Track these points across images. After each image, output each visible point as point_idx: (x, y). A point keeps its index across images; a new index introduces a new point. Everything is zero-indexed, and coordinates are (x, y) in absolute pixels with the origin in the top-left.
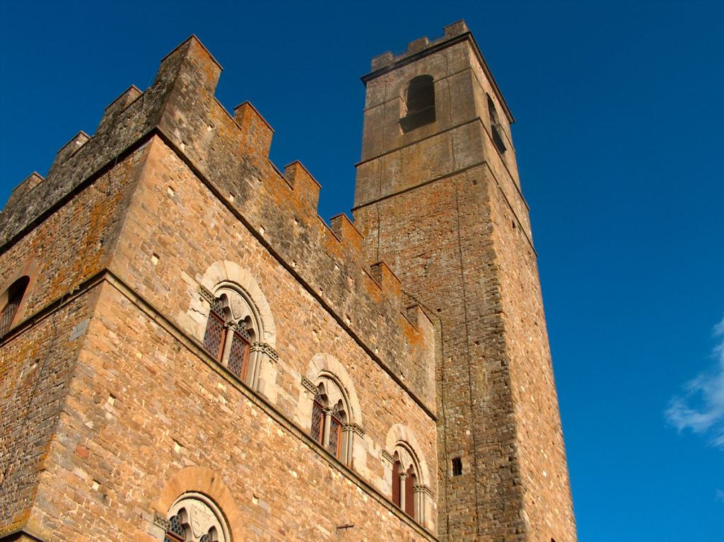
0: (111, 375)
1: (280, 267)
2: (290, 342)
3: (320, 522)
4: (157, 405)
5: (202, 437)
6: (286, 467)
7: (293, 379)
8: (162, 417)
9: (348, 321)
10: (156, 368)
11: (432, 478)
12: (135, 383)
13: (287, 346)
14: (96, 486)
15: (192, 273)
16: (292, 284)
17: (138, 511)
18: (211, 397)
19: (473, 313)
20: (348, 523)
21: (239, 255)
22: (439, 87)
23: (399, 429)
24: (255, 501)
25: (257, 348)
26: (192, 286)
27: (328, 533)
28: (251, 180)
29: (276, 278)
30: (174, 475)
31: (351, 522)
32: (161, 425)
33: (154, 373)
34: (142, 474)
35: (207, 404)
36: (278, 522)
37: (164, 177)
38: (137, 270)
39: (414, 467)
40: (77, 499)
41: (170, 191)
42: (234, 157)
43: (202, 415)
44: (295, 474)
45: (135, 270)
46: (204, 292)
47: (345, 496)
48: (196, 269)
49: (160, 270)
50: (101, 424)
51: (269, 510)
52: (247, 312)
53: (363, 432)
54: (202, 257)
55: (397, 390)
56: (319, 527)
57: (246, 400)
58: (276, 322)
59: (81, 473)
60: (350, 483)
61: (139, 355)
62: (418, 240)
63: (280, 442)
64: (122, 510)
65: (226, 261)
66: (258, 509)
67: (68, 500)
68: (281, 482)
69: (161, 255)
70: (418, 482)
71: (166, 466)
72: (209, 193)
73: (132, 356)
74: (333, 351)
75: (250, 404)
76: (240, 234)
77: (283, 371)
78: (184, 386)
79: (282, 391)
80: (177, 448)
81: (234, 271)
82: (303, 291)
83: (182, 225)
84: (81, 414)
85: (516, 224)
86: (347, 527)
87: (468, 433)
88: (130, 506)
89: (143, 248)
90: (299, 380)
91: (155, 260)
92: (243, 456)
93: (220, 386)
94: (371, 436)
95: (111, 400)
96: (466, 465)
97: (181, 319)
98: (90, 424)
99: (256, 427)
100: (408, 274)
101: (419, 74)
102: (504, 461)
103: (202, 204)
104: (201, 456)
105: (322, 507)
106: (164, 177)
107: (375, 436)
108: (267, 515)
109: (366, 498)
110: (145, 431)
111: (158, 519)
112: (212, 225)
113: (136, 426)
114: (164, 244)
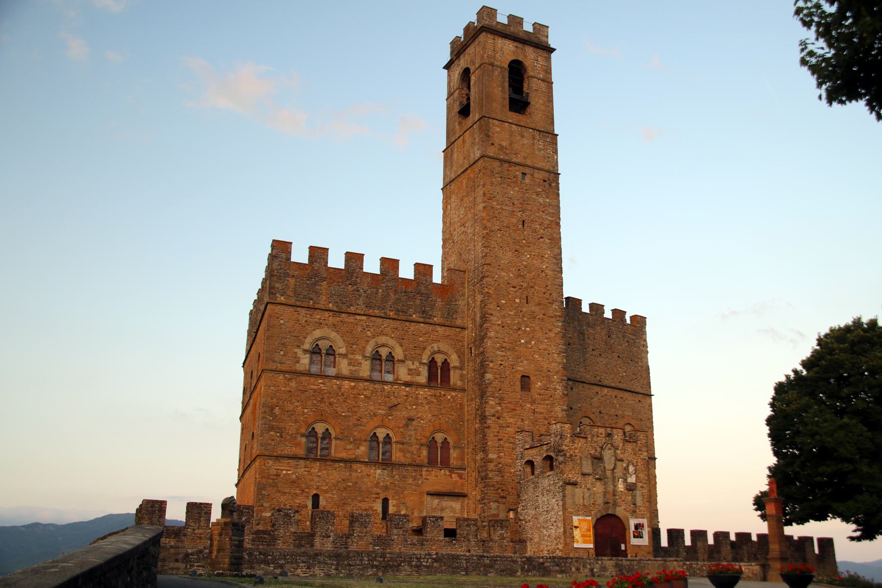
0: (275, 400)
1: (343, 315)
2: (353, 344)
3: (379, 409)
4: (294, 400)
5: (315, 402)
6: (357, 396)
7: (357, 359)
8: (297, 404)
9: (391, 313)
10: (291, 389)
11: (462, 362)
12: (284, 398)
13: (352, 347)
14: (278, 434)
15: (299, 347)
16: (351, 319)
17: (294, 435)
18: (316, 387)
20: (397, 403)
21: (319, 325)
23: (432, 347)
24: (343, 414)
27: (384, 412)
28: (321, 285)
29: (341, 321)
30: (306, 420)
31: (398, 402)
32: (297, 406)
33: (291, 391)
34: (293, 424)
35: (315, 391)
36: (356, 417)
37: (278, 318)
39: (448, 359)
40: (273, 440)
41: (282, 322)
42: (308, 282)
43: (313, 395)
44: (363, 396)
46: (305, 351)
47: (394, 393)
49: (284, 355)
50: (275, 417)
51: (350, 414)
53: (404, 361)
54: (301, 338)
55: (431, 328)
56: (378, 411)
58: (344, 341)
59: (272, 433)
60: (397, 387)
61: (283, 389)
63: (354, 388)
64: (288, 437)
65: (314, 332)
66: (345, 416)
67: (270, 442)
68: (356, 402)
70: (451, 365)
71: (302, 418)
72: (299, 309)
73: (281, 390)
74: (382, 333)
76: (318, 316)
77: (351, 359)
78: (304, 389)
79: (351, 367)
80: (306, 411)
81: (318, 333)
82: (358, 317)
83: (290, 331)
84: (268, 417)
85: (527, 170)
86: (395, 406)
87: (474, 334)
88: (291, 435)
89: (276, 352)
90: (361, 358)
91: (282, 353)
92: (335, 401)
93: (320, 381)
94: (410, 360)
95: (277, 408)
96: (473, 351)
98: (271, 419)
99: (340, 388)
102: (481, 349)
104: (316, 409)
105: (380, 403)
107: (413, 359)
108: (349, 416)
109: (407, 389)
110: (292, 411)
111: (303, 435)
112: (304, 321)
113: (288, 411)
114: (283, 344)
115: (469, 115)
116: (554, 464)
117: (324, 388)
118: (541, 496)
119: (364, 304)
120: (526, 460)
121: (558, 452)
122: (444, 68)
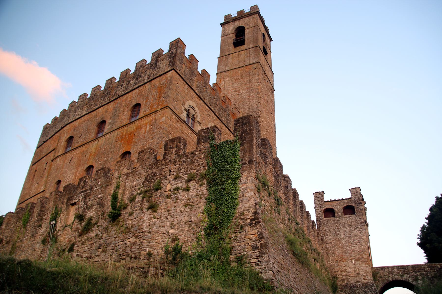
1: (201, 101)
10: (177, 128)
15: (183, 105)
16: (204, 105)
18: (188, 134)
19: (251, 111)
21: (192, 99)
22: (247, 32)
25: (196, 122)
26: (183, 108)
33: (177, 129)
37: (176, 81)
38: (172, 105)
41: (177, 84)
45: (172, 105)
46: (185, 109)
48: (183, 103)
52: (194, 113)
57: (194, 134)
58: (200, 115)
61: (174, 125)
62: (237, 86)
69: (177, 101)
72: (185, 83)
75: (195, 135)
81: (191, 103)
82: (206, 106)
85: (268, 81)
91: (176, 102)
93: (189, 131)
95: (170, 135)
97: (181, 116)
100: (233, 97)
101: (240, 25)
103: (184, 86)
106: (176, 81)
112: (186, 92)
114: (177, 98)
115: (244, 44)
116: (355, 210)
117: (191, 137)
118: (342, 228)
119: (209, 101)
120: (325, 208)
121: (359, 203)
122: (220, 24)
